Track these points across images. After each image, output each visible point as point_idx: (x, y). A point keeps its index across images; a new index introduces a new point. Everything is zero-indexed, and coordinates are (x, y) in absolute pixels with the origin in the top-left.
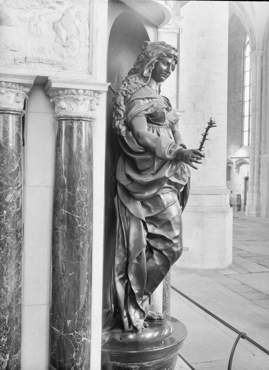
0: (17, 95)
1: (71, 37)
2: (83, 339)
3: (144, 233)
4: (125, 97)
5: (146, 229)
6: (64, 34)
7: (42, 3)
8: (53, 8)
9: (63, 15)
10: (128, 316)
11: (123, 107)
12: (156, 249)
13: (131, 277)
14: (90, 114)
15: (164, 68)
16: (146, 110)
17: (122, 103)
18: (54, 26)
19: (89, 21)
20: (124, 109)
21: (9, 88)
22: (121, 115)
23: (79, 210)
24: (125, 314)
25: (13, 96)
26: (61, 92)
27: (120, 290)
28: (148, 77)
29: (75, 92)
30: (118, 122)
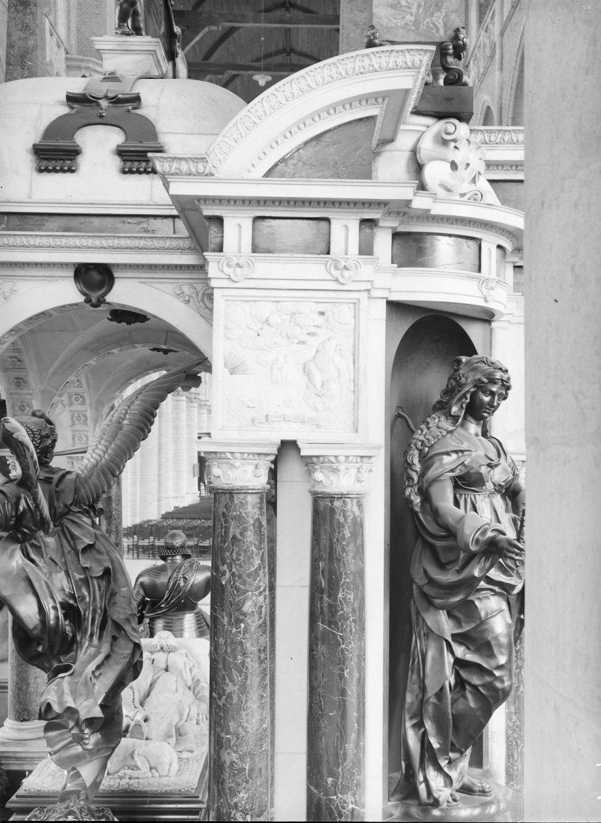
0: (256, 467)
1: (328, 381)
3: (449, 659)
4: (421, 451)
7: (288, 338)
8: (303, 343)
10: (426, 781)
11: (418, 467)
12: (470, 684)
13: (429, 725)
15: (487, 399)
16: (452, 471)
17: (416, 460)
18: (304, 368)
19: (354, 355)
20: (418, 470)
21: (244, 459)
22: (413, 479)
23: (342, 625)
24: (421, 778)
25: (251, 469)
26: (315, 460)
28: (459, 417)
29: (333, 459)
30: (410, 489)
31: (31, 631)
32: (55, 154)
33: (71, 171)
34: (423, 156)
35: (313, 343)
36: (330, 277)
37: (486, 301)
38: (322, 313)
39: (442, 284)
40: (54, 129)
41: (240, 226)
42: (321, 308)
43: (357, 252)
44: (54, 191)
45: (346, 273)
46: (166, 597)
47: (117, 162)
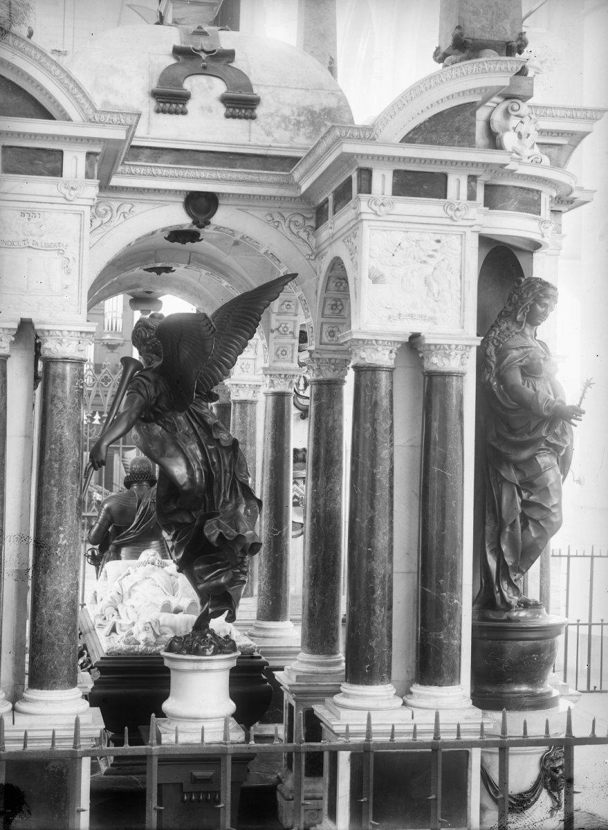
1: (443, 291)
2: (455, 601)
3: (518, 500)
4: (497, 347)
5: (520, 495)
6: (435, 288)
7: (414, 258)
8: (425, 262)
9: (435, 268)
10: (500, 591)
11: (494, 359)
12: (531, 519)
13: (504, 548)
14: (461, 369)
16: (521, 361)
17: (493, 354)
18: (425, 281)
19: (461, 273)
20: (495, 360)
21: (385, 345)
22: (492, 368)
23: (451, 468)
26: (433, 347)
27: (492, 564)
28: (522, 322)
29: (447, 347)
30: (489, 375)
31: (182, 486)
32: (170, 99)
33: (184, 113)
34: (495, 127)
35: (432, 262)
36: (446, 215)
37: (543, 236)
38: (438, 241)
39: (510, 225)
40: (167, 77)
41: (384, 176)
42: (438, 237)
43: (391, 193)
44: (165, 130)
45: (458, 213)
46: (135, 523)
47: (222, 109)
